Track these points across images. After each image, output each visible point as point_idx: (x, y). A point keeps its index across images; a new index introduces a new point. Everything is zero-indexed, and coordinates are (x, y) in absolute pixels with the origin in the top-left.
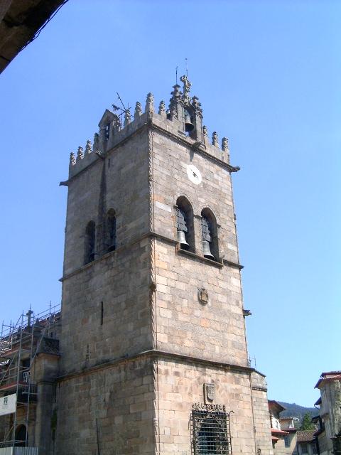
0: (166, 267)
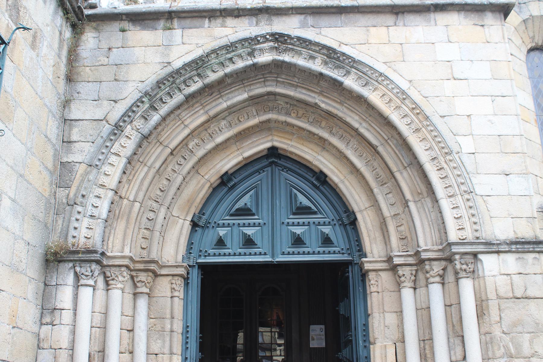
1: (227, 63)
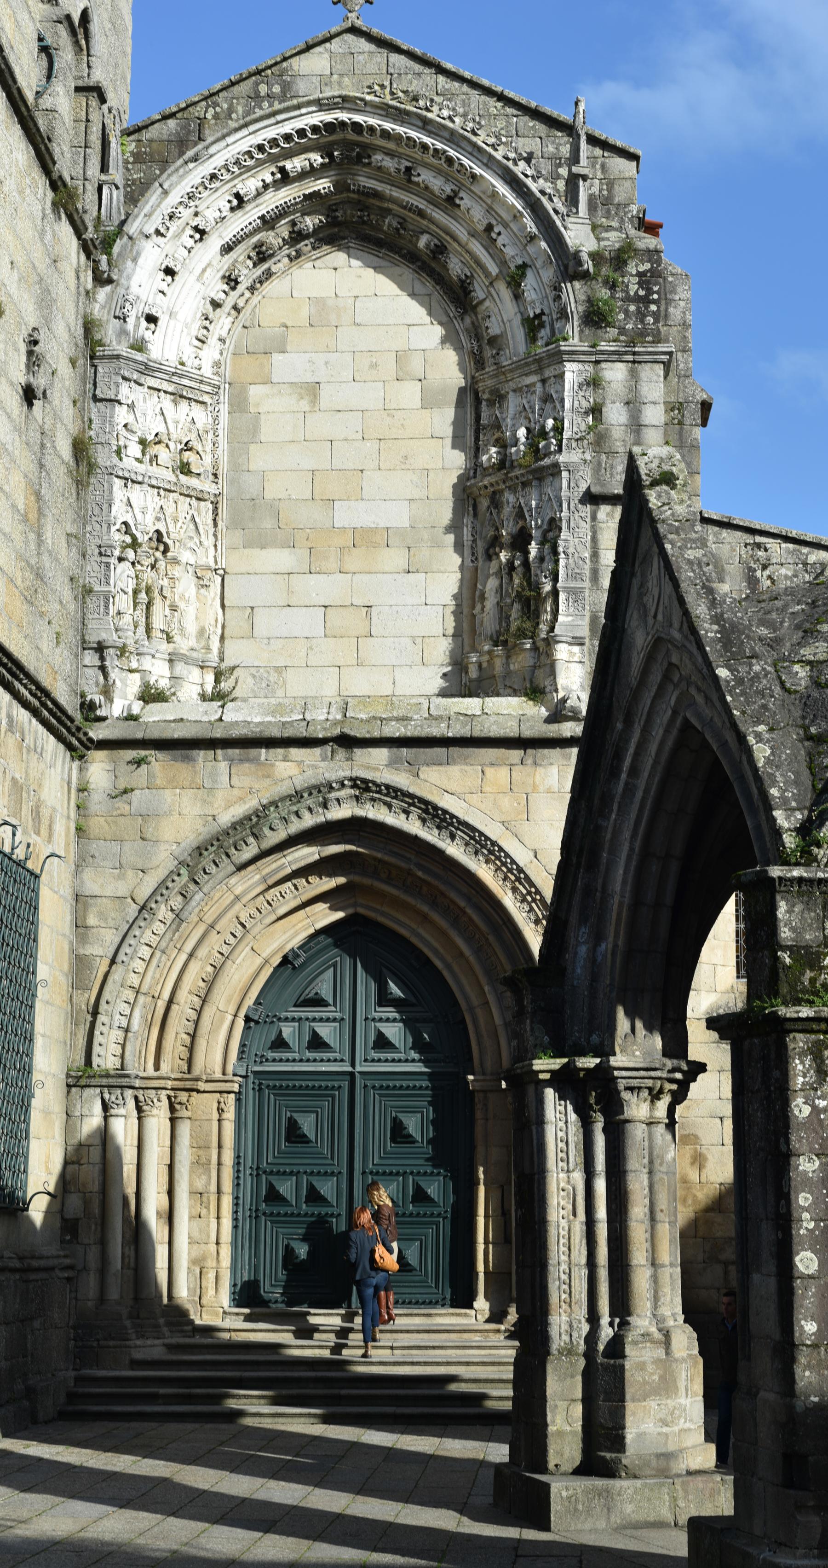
1: (293, 818)
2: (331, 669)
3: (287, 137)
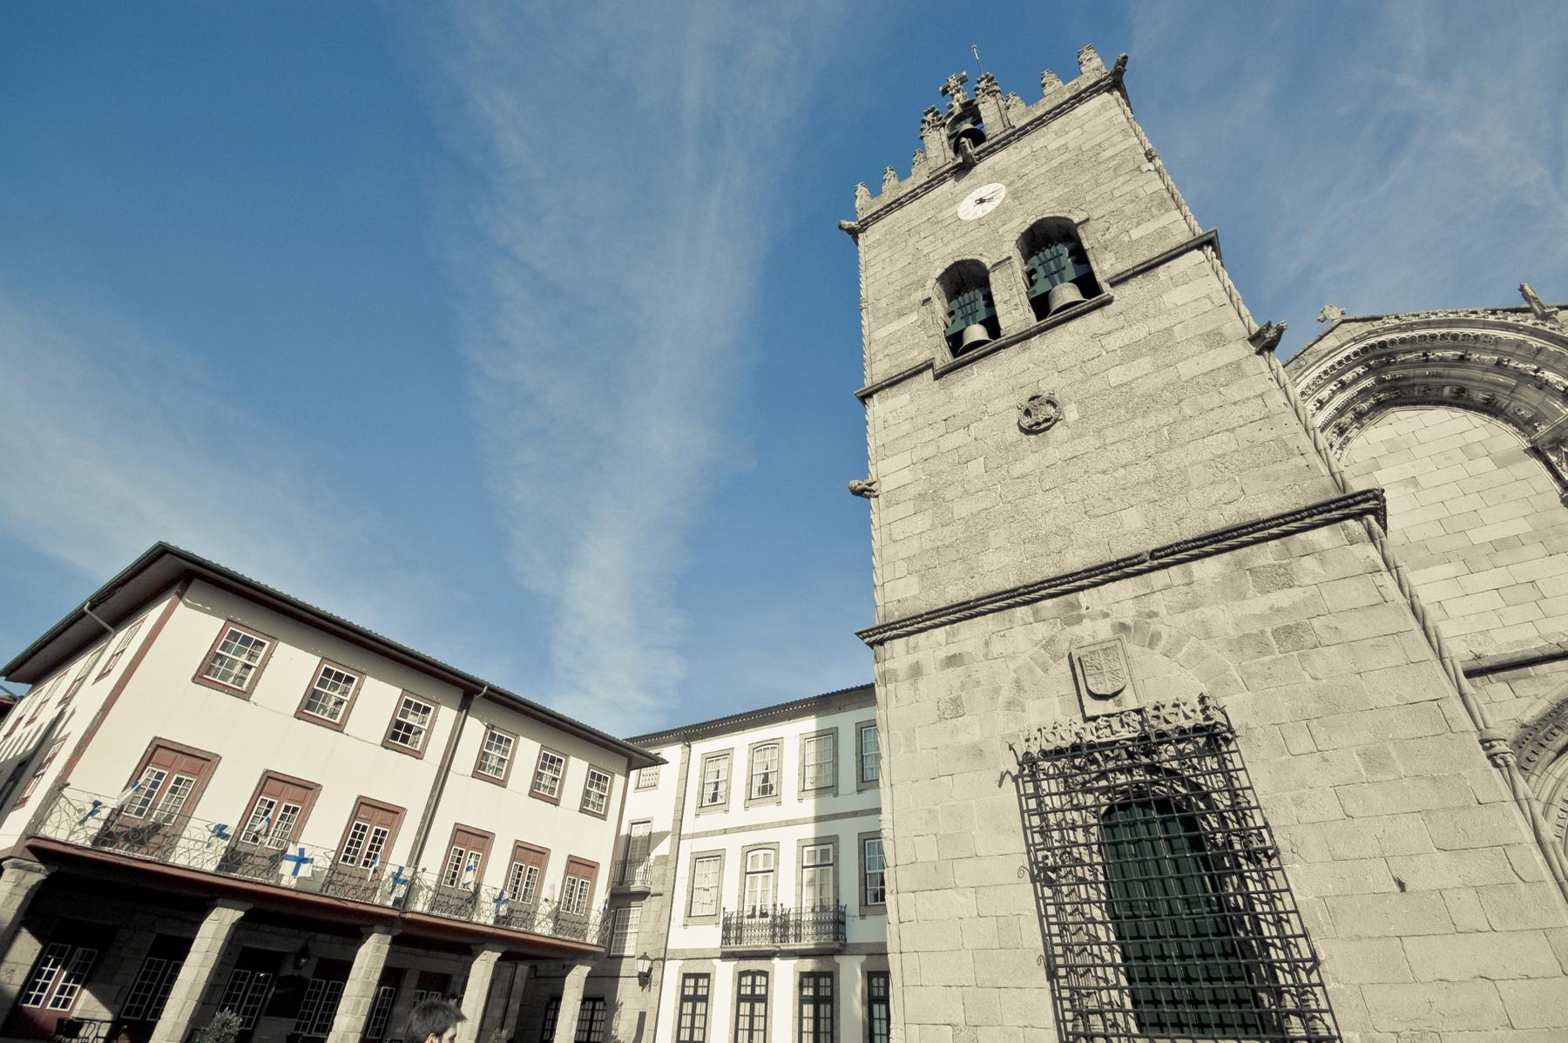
0: (906, 427)
2: (1526, 625)
3: (1340, 363)
